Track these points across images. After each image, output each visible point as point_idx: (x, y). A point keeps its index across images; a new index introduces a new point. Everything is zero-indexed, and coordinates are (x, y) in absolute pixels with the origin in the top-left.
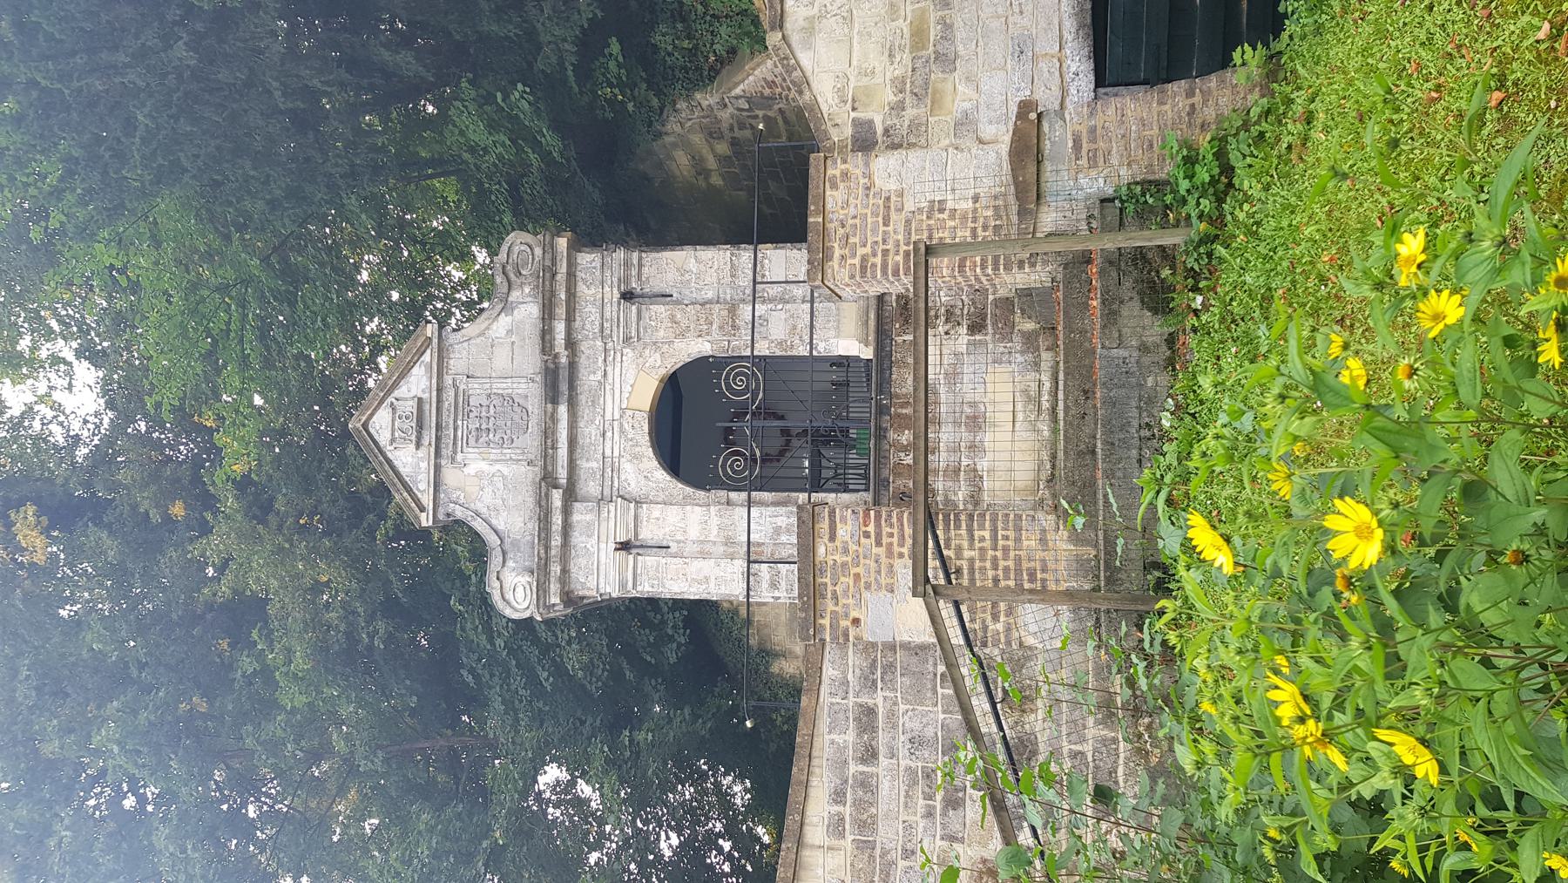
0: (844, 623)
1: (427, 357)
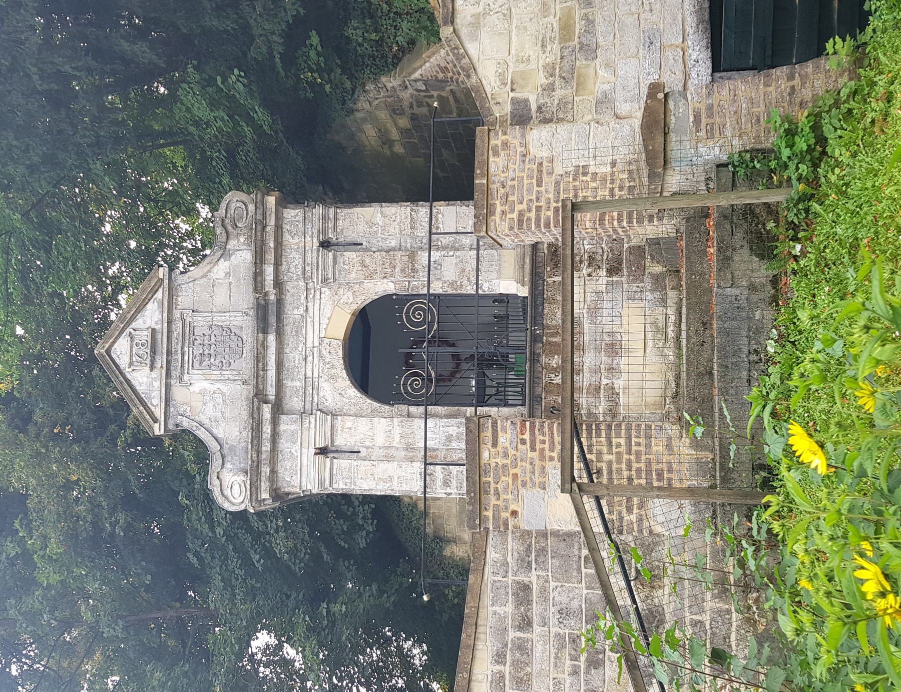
0: (505, 515)
1: (159, 295)
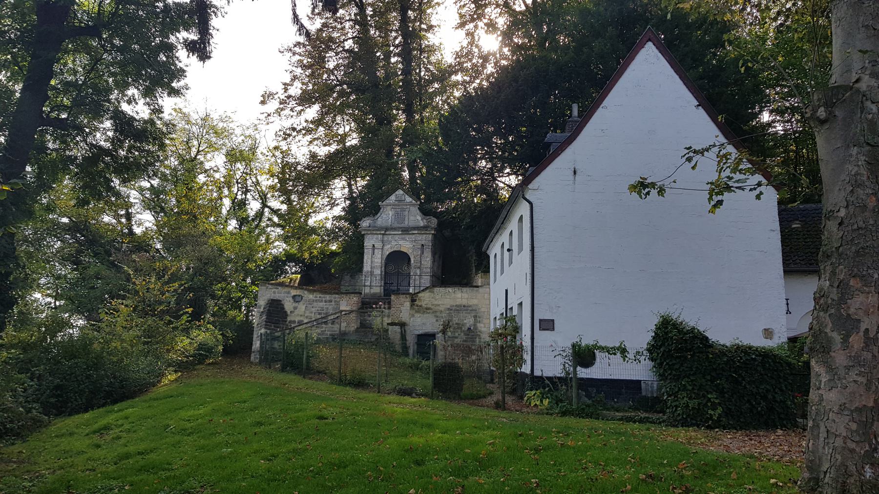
1: (414, 202)
